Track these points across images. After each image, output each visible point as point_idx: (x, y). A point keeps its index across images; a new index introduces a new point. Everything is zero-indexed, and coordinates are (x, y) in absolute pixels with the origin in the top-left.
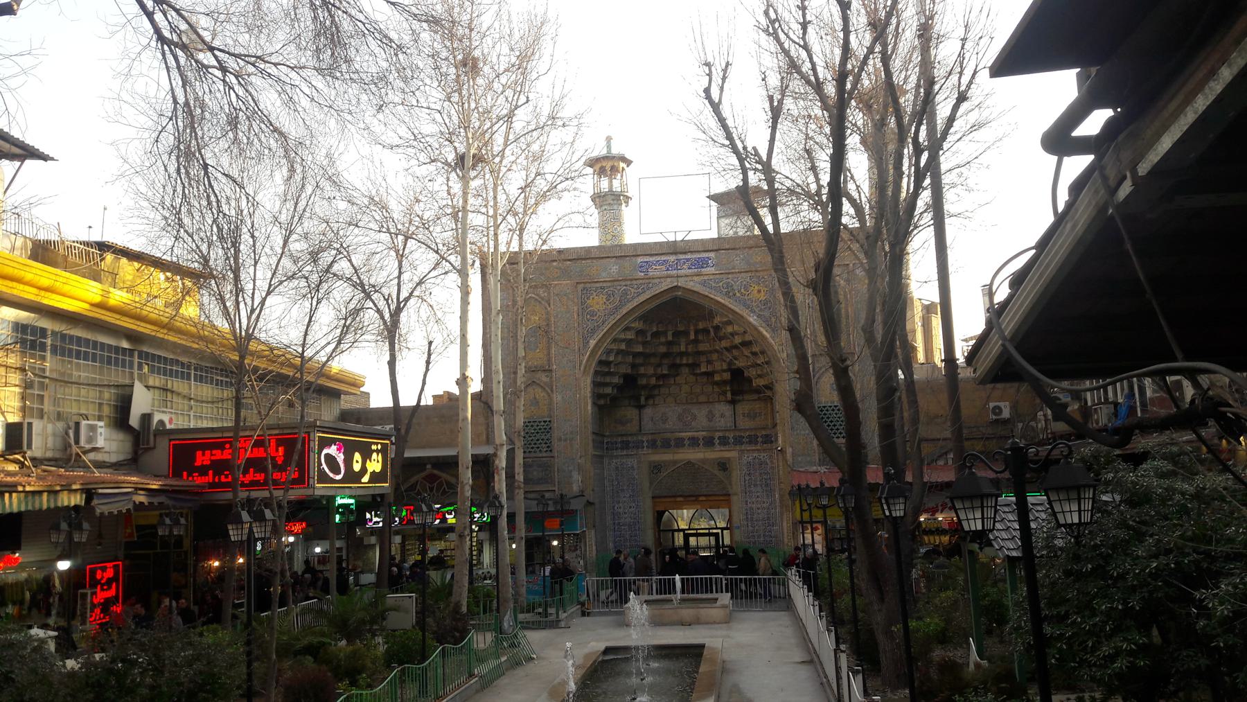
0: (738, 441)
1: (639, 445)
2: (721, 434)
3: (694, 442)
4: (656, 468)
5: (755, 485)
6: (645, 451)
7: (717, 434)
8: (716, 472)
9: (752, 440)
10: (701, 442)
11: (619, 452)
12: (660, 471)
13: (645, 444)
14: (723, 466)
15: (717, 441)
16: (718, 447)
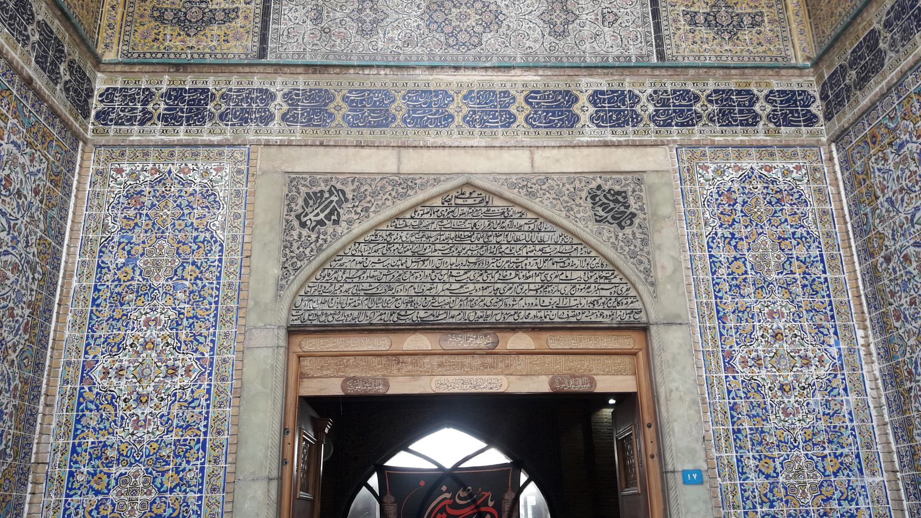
0: (677, 111)
1: (247, 110)
2: (601, 83)
3: (491, 111)
4: (317, 203)
5: (763, 286)
6: (276, 130)
7: (588, 84)
8: (587, 229)
9: (734, 109)
10: (520, 109)
11: (156, 133)
12: (333, 216)
13: (278, 107)
14: (615, 204)
15: (584, 109)
16: (591, 133)
